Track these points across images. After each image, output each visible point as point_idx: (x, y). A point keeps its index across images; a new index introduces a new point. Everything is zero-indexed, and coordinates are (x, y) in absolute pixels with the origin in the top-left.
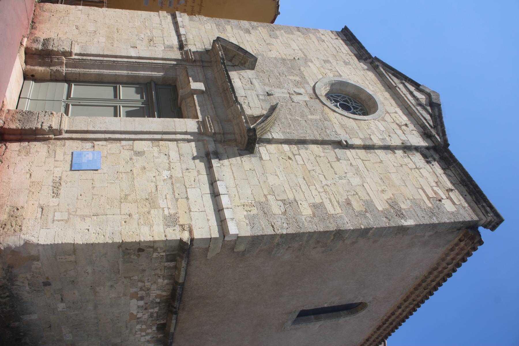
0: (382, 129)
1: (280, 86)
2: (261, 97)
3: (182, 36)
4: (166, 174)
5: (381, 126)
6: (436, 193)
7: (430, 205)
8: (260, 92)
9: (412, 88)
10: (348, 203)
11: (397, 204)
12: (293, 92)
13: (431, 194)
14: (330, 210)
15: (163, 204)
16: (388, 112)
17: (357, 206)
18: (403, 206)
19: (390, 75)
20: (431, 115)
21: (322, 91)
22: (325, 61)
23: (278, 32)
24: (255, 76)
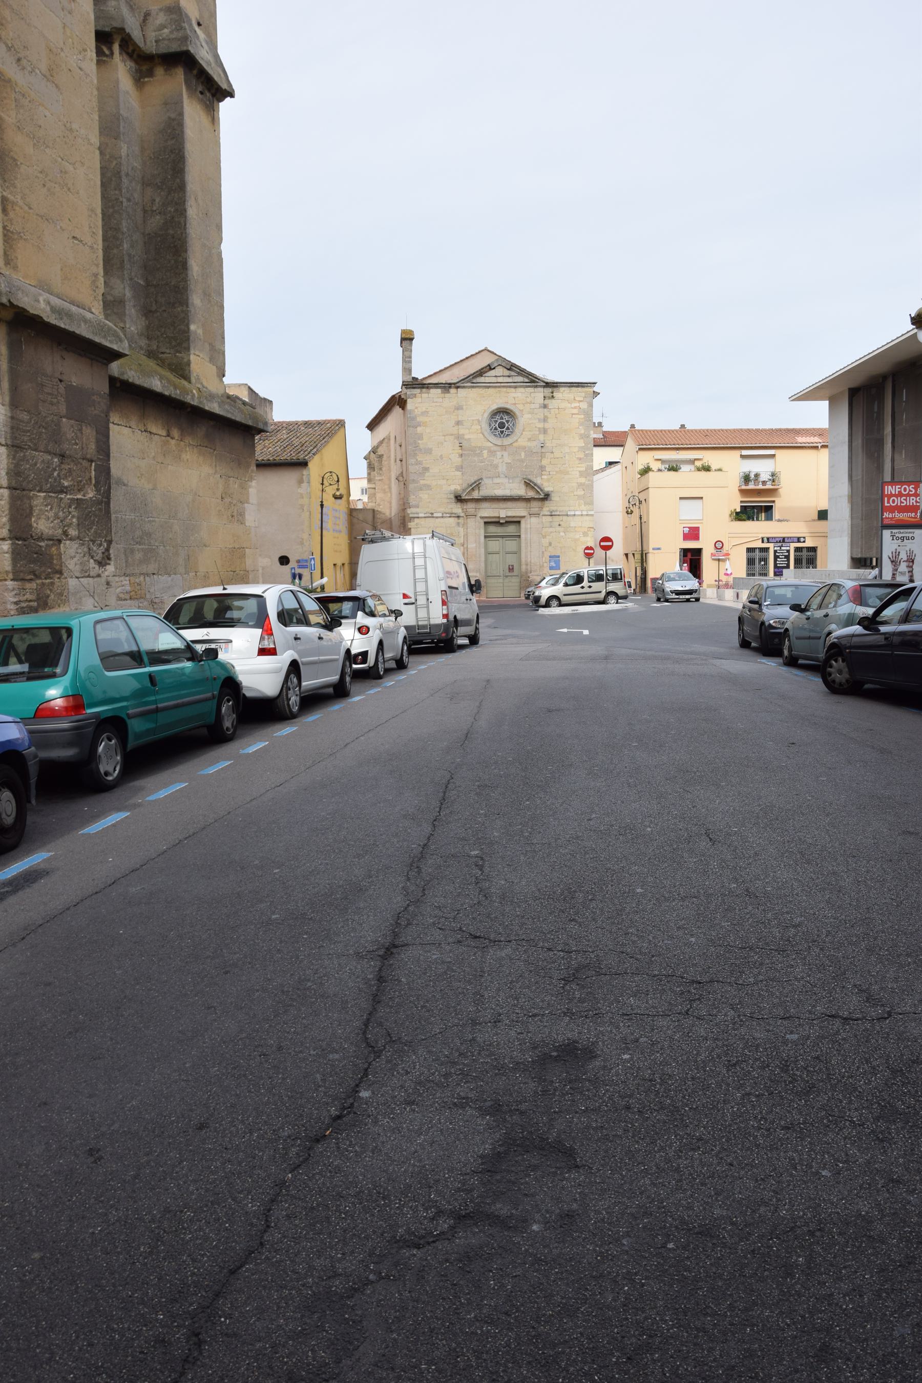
0: (530, 416)
1: (496, 466)
2: (511, 481)
3: (445, 515)
4: (562, 534)
5: (527, 416)
6: (575, 408)
7: (583, 416)
8: (506, 480)
9: (492, 373)
10: (580, 459)
11: (581, 435)
12: (501, 460)
13: (575, 411)
14: (583, 469)
15: (577, 537)
16: (515, 404)
17: (582, 455)
18: (583, 432)
19: (474, 381)
20: (519, 374)
21: (499, 441)
22: (458, 423)
23: (421, 446)
24: (490, 480)
